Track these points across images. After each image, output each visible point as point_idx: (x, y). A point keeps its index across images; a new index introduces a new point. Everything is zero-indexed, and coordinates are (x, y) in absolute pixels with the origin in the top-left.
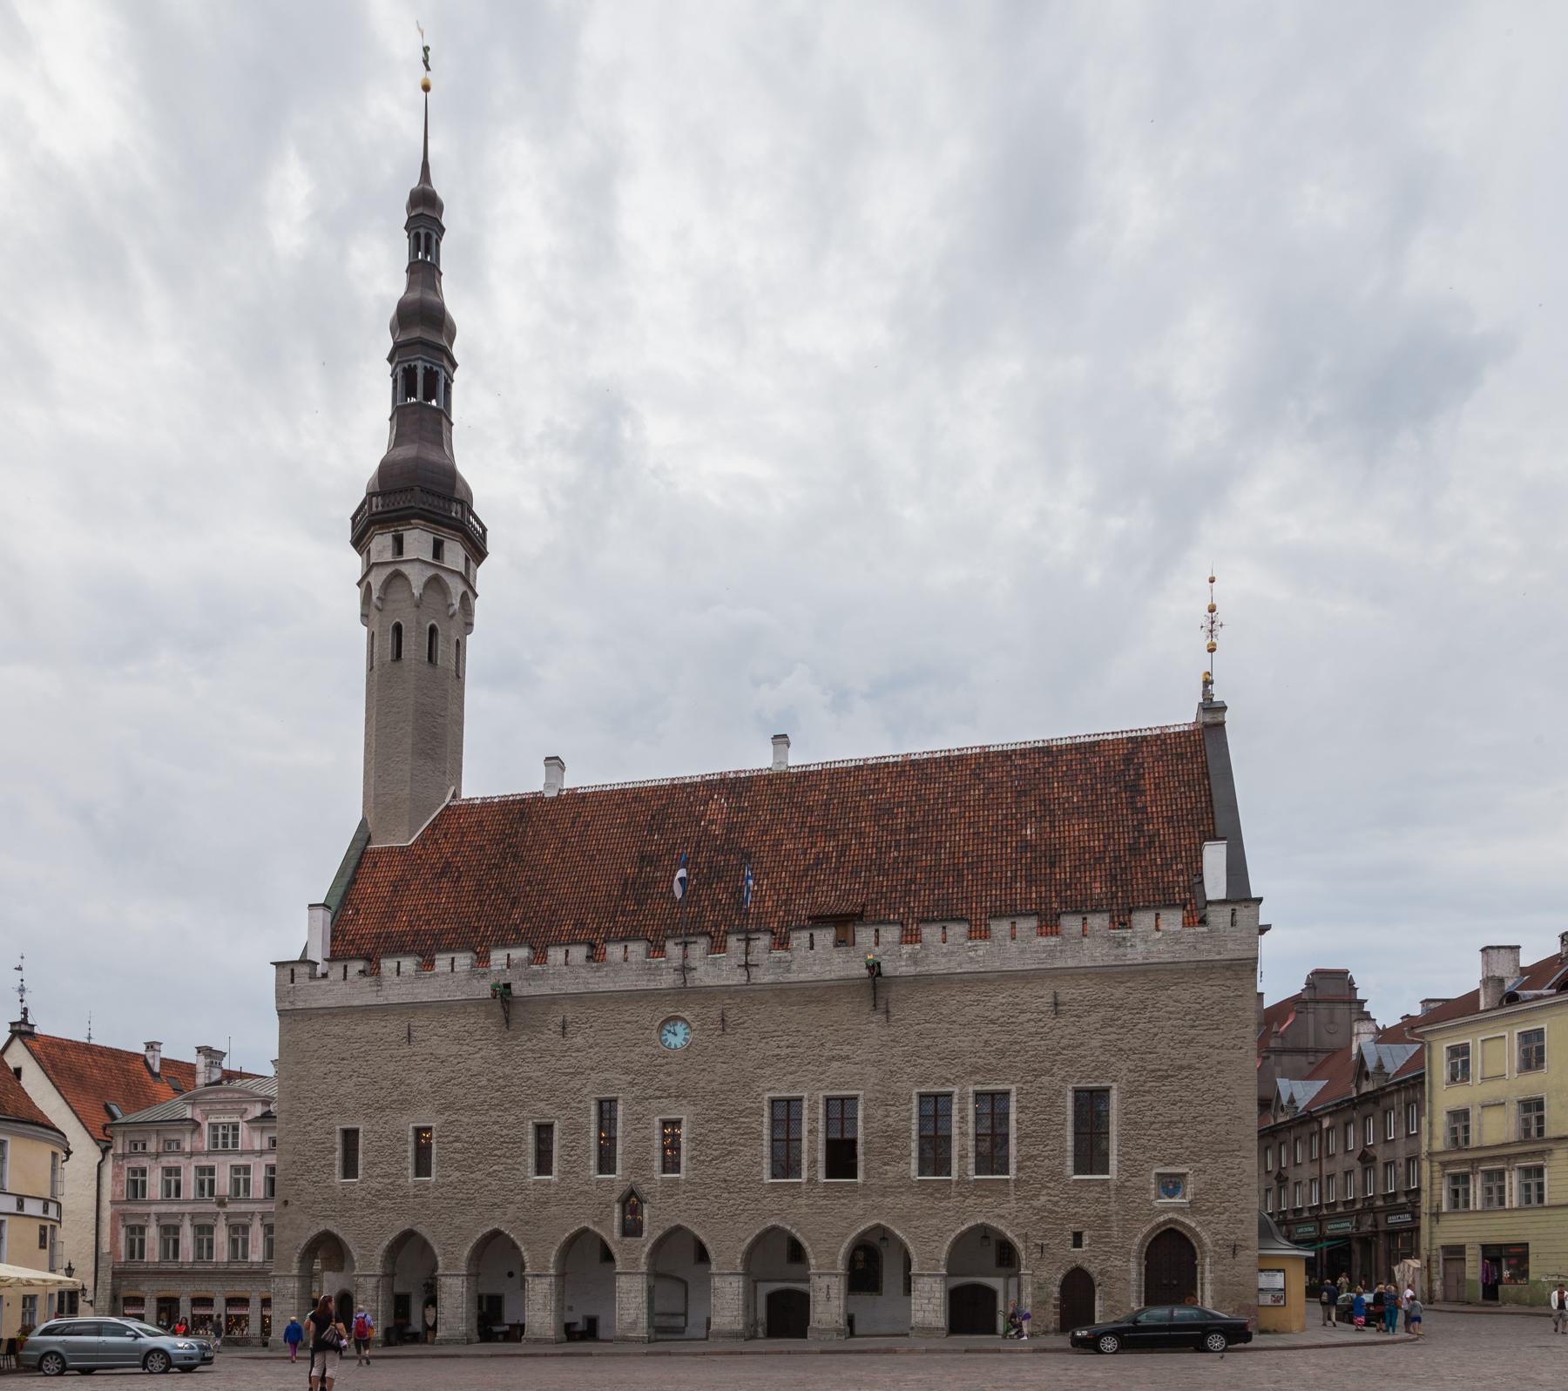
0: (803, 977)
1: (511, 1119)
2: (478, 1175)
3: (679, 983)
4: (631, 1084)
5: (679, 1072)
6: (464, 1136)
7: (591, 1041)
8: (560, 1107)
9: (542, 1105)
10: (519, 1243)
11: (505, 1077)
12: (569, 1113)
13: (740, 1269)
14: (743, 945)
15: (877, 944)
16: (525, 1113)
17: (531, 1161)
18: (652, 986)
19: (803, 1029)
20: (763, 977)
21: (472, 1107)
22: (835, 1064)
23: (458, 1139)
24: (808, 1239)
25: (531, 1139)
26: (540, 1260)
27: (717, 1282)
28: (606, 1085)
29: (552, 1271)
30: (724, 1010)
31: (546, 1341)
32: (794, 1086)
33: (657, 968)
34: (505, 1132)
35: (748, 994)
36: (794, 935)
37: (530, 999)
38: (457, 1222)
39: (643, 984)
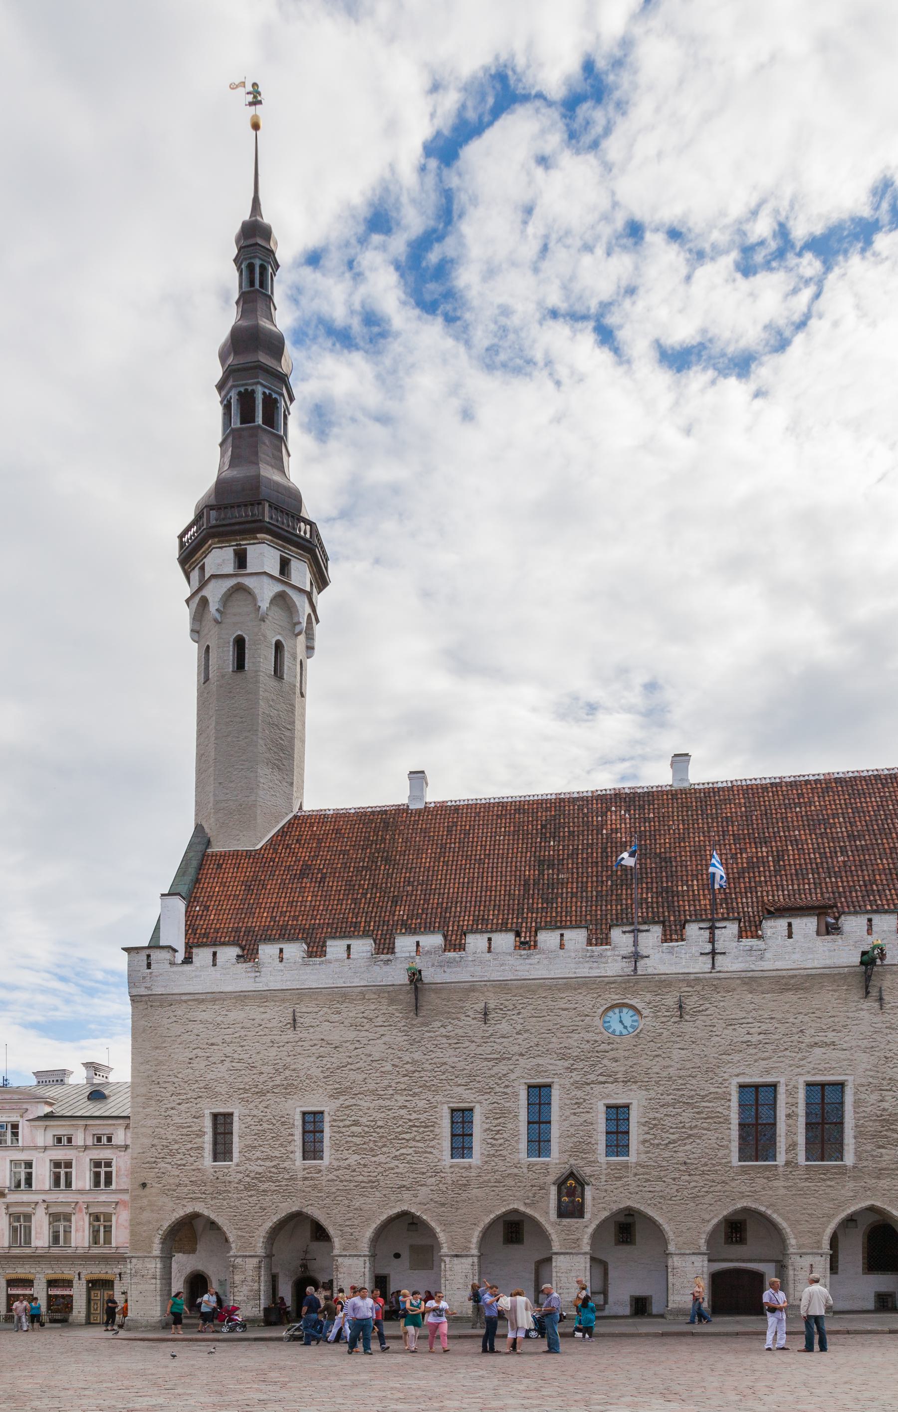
0: (779, 965)
1: (422, 1104)
3: (629, 970)
4: (570, 1069)
5: (627, 1058)
7: (519, 1027)
8: (481, 1092)
9: (460, 1090)
11: (414, 1062)
14: (706, 934)
18: (595, 973)
19: (779, 1016)
20: (728, 964)
23: (356, 1123)
28: (538, 1070)
30: (682, 1000)
32: (768, 1072)
33: (601, 956)
34: (414, 1116)
35: (714, 984)
36: (766, 924)
37: (440, 988)
38: (357, 1204)
39: (585, 971)
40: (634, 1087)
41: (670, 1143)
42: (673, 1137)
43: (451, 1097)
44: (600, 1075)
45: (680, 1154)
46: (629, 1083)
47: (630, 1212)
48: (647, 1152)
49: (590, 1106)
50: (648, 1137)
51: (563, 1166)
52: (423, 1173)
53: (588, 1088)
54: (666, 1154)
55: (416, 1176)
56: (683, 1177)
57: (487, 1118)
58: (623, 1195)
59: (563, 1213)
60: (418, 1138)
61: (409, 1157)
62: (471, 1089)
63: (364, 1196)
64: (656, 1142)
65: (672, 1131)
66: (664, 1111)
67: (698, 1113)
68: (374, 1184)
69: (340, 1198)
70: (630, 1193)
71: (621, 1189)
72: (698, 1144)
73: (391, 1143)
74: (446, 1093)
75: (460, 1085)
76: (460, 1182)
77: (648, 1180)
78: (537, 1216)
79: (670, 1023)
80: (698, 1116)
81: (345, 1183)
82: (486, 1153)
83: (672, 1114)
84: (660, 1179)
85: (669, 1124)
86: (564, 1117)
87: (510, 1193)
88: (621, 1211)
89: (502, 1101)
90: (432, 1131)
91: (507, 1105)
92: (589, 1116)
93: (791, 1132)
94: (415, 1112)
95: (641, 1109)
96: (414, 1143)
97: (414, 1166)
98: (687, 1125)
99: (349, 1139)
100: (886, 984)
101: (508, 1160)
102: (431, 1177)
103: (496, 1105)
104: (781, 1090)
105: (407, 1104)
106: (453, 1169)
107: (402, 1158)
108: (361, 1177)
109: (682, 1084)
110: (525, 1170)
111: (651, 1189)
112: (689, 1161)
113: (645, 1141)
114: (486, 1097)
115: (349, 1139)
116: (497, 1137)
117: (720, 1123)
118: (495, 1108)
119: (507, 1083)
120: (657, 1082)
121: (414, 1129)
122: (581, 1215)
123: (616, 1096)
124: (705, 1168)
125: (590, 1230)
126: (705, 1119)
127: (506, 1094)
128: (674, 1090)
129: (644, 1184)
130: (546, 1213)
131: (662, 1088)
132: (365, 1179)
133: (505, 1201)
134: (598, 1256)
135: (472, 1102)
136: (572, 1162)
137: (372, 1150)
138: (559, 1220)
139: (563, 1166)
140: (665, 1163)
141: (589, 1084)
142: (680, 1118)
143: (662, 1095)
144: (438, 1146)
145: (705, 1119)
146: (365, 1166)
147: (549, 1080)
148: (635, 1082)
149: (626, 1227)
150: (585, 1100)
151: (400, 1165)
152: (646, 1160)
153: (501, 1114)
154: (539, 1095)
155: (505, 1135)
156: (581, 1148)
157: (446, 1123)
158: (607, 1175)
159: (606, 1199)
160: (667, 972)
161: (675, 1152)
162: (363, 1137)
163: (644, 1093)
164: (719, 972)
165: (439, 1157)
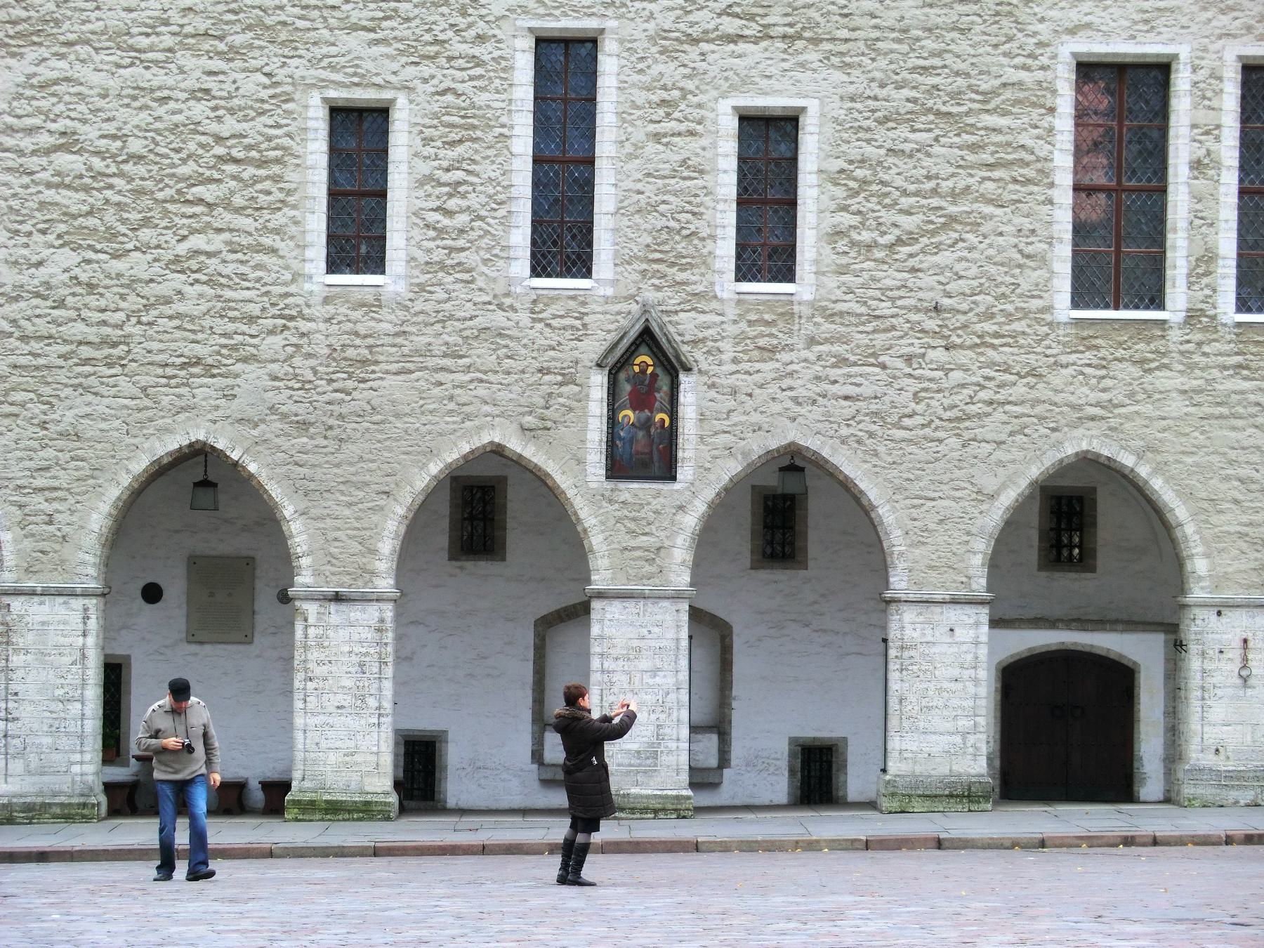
1: (252, 85)
2: (137, 265)
6: (89, 133)
8: (414, 53)
9: (354, 42)
10: (275, 491)
12: (445, 76)
13: (980, 584)
16: (298, 67)
17: (317, 224)
21: (119, 38)
23: (69, 141)
24: (1187, 495)
25: (316, 152)
26: (347, 530)
27: (907, 625)
29: (385, 584)
31: (366, 811)
34: (230, 125)
38: (66, 417)
40: (812, 56)
41: (900, 241)
42: (909, 223)
43: (331, 67)
44: (726, 12)
45: (927, 280)
46: (800, 44)
47: (794, 463)
48: (842, 270)
49: (697, 114)
50: (846, 219)
51: (624, 307)
52: (252, 320)
53: (693, 52)
54: (891, 277)
55: (231, 327)
56: (932, 354)
57: (427, 141)
58: (776, 408)
59: (620, 466)
60: (238, 201)
61: (213, 263)
62: (384, 41)
63: (87, 389)
64: (866, 236)
65: (905, 202)
66: (881, 134)
67: (974, 148)
68: (113, 350)
69: (19, 396)
70: (796, 400)
71: (773, 389)
72: (971, 249)
73: (166, 213)
74: (318, 51)
75: (355, 28)
76: (351, 353)
77: (842, 361)
78: (551, 467)
80: (971, 158)
81: (35, 346)
82: (422, 257)
83: (907, 147)
84: (872, 357)
85: (899, 182)
86: (628, 148)
87: (482, 391)
88: (771, 457)
89: (466, 87)
90: (276, 179)
91: (482, 98)
92: (695, 144)
93: (1202, 221)
94: (232, 111)
95: (829, 129)
96: (228, 216)
97: (228, 294)
98: (946, 186)
99: (49, 195)
101: (480, 282)
102: (271, 332)
103: (450, 98)
104: (1181, 81)
105: (210, 83)
106: (331, 309)
107: (193, 264)
108: (80, 326)
109: (933, 54)
110: (524, 318)
111: (852, 390)
112: (946, 302)
113: (838, 233)
114: (426, 69)
115: (49, 195)
116: (452, 204)
117: (1029, 181)
118: (447, 110)
119: (481, 27)
120: (871, 43)
121: (230, 168)
122: (669, 474)
123: (764, 83)
124: (989, 327)
125: (691, 521)
126: (990, 166)
127: (477, 62)
128: (913, 70)
129: (834, 373)
130: (574, 460)
131: (882, 63)
132: (92, 333)
133: (468, 417)
134: (711, 605)
135: (387, 85)
136: (650, 295)
137: (113, 235)
138: (610, 485)
139: (624, 307)
140: (885, 308)
141: (695, 41)
142: (927, 162)
143: (882, 86)
144: (293, 229)
145: (990, 166)
146: (91, 287)
147: (590, 24)
148: (816, 41)
149: (784, 514)
150: (685, 93)
151: (188, 289)
152: (839, 294)
153: (463, 127)
154: (566, 67)
155: (473, 201)
156: (669, 253)
157: (317, 151)
158: (739, 339)
159: (735, 418)
161: (914, 270)
162: (87, 189)
163: (838, 76)
165: (295, 265)
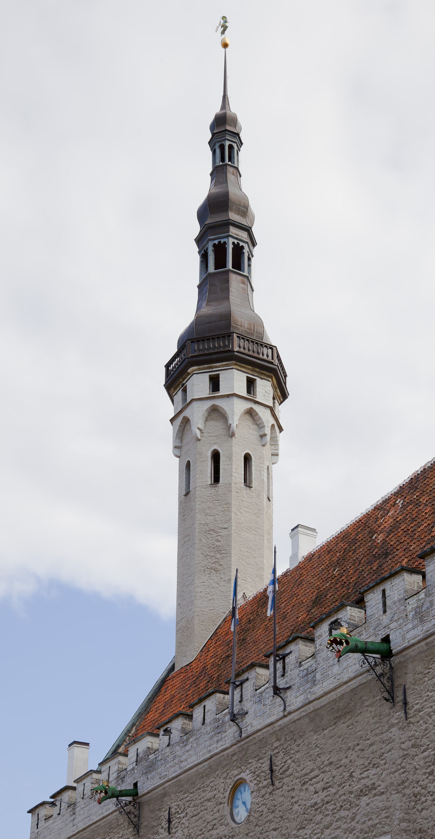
15: (385, 612)
22: (365, 800)
79: (267, 796)
100: (410, 678)
160: (259, 727)
164: (290, 713)
